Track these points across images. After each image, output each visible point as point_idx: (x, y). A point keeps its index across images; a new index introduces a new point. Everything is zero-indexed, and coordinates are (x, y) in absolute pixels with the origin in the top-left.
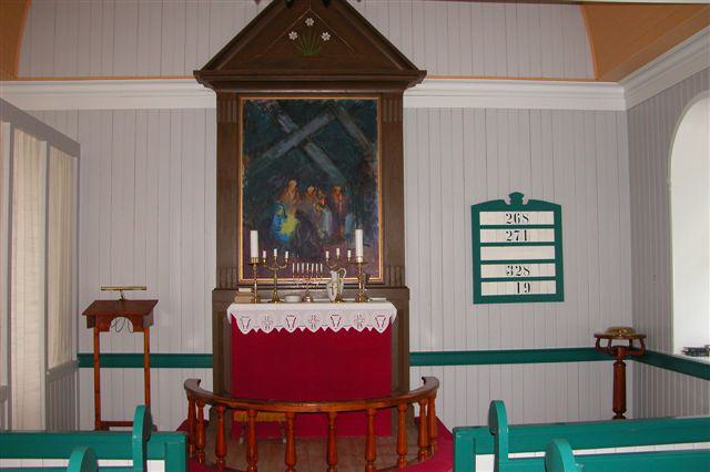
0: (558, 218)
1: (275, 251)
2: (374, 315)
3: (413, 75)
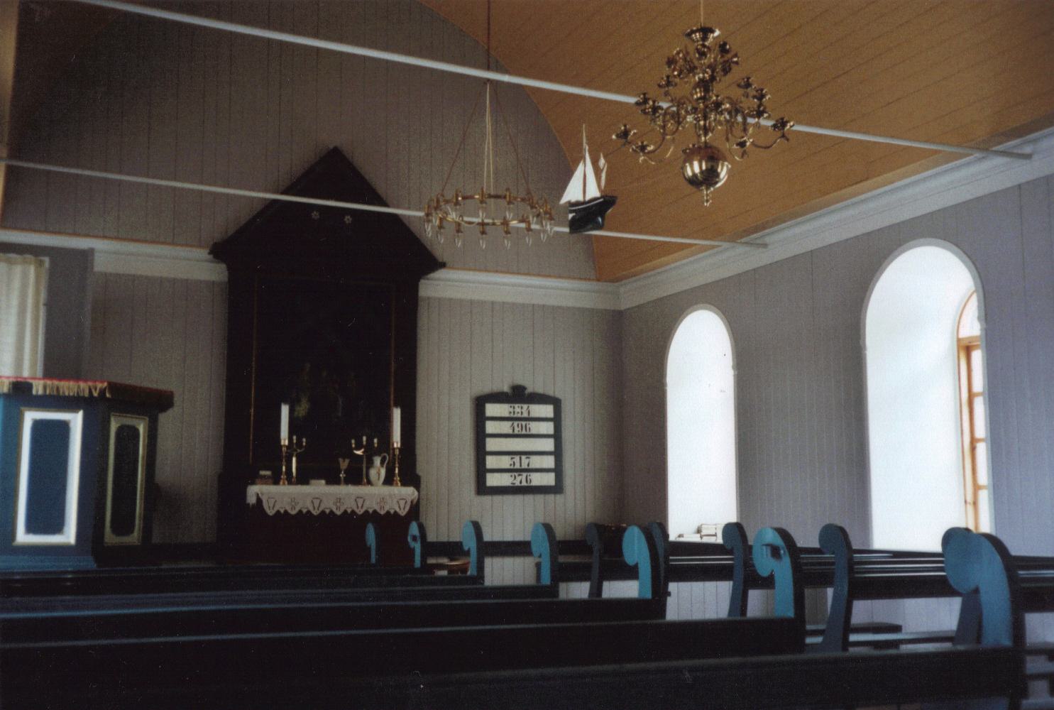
0: (558, 411)
1: (353, 441)
2: (397, 497)
3: (431, 264)
